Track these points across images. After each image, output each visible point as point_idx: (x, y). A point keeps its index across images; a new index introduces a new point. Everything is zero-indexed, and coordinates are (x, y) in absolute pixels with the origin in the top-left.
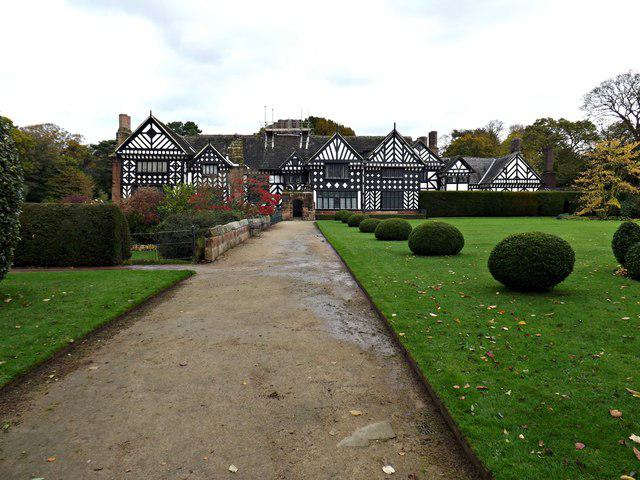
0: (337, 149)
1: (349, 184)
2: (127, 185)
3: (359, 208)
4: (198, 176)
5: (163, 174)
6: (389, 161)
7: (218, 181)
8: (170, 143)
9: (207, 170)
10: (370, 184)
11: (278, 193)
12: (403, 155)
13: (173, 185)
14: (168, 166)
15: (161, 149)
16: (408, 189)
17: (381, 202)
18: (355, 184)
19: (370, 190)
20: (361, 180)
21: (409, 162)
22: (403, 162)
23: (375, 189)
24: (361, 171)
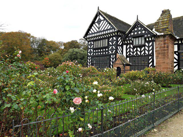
2: (89, 56)
4: (130, 47)
5: (105, 48)
7: (145, 50)
8: (108, 24)
9: (138, 42)
13: (111, 55)
14: (108, 42)
15: (104, 31)
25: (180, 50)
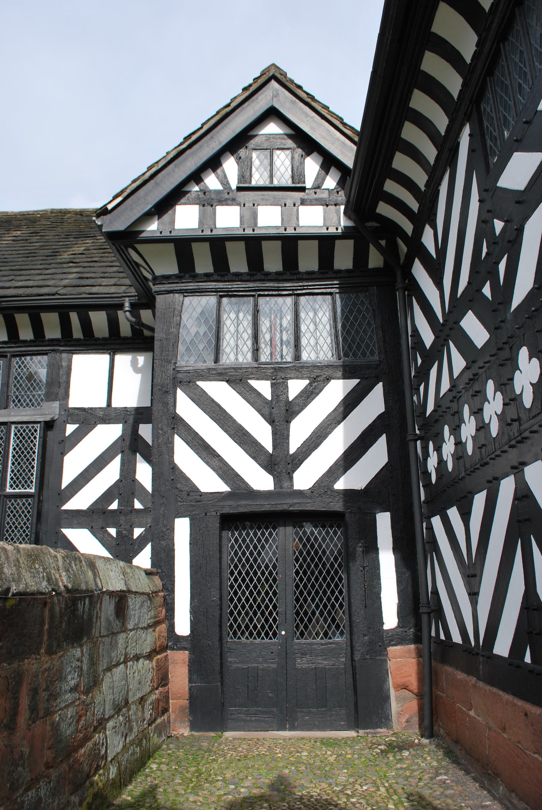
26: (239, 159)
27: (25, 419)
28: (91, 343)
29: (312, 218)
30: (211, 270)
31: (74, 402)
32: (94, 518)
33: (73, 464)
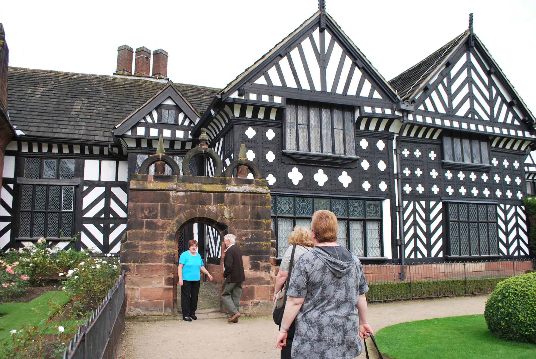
0: (323, 59)
1: (358, 176)
3: (388, 254)
6: (461, 112)
10: (413, 180)
11: (107, 209)
12: (491, 103)
16: (504, 199)
17: (445, 236)
18: (374, 176)
19: (414, 197)
20: (389, 164)
21: (504, 125)
22: (493, 122)
23: (428, 196)
24: (387, 137)
25: (22, 176)
26: (157, 112)
27: (68, 184)
28: (92, 156)
29: (180, 134)
30: (146, 146)
31: (86, 178)
32: (95, 220)
33: (87, 201)
